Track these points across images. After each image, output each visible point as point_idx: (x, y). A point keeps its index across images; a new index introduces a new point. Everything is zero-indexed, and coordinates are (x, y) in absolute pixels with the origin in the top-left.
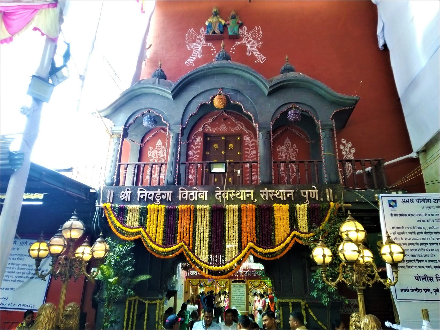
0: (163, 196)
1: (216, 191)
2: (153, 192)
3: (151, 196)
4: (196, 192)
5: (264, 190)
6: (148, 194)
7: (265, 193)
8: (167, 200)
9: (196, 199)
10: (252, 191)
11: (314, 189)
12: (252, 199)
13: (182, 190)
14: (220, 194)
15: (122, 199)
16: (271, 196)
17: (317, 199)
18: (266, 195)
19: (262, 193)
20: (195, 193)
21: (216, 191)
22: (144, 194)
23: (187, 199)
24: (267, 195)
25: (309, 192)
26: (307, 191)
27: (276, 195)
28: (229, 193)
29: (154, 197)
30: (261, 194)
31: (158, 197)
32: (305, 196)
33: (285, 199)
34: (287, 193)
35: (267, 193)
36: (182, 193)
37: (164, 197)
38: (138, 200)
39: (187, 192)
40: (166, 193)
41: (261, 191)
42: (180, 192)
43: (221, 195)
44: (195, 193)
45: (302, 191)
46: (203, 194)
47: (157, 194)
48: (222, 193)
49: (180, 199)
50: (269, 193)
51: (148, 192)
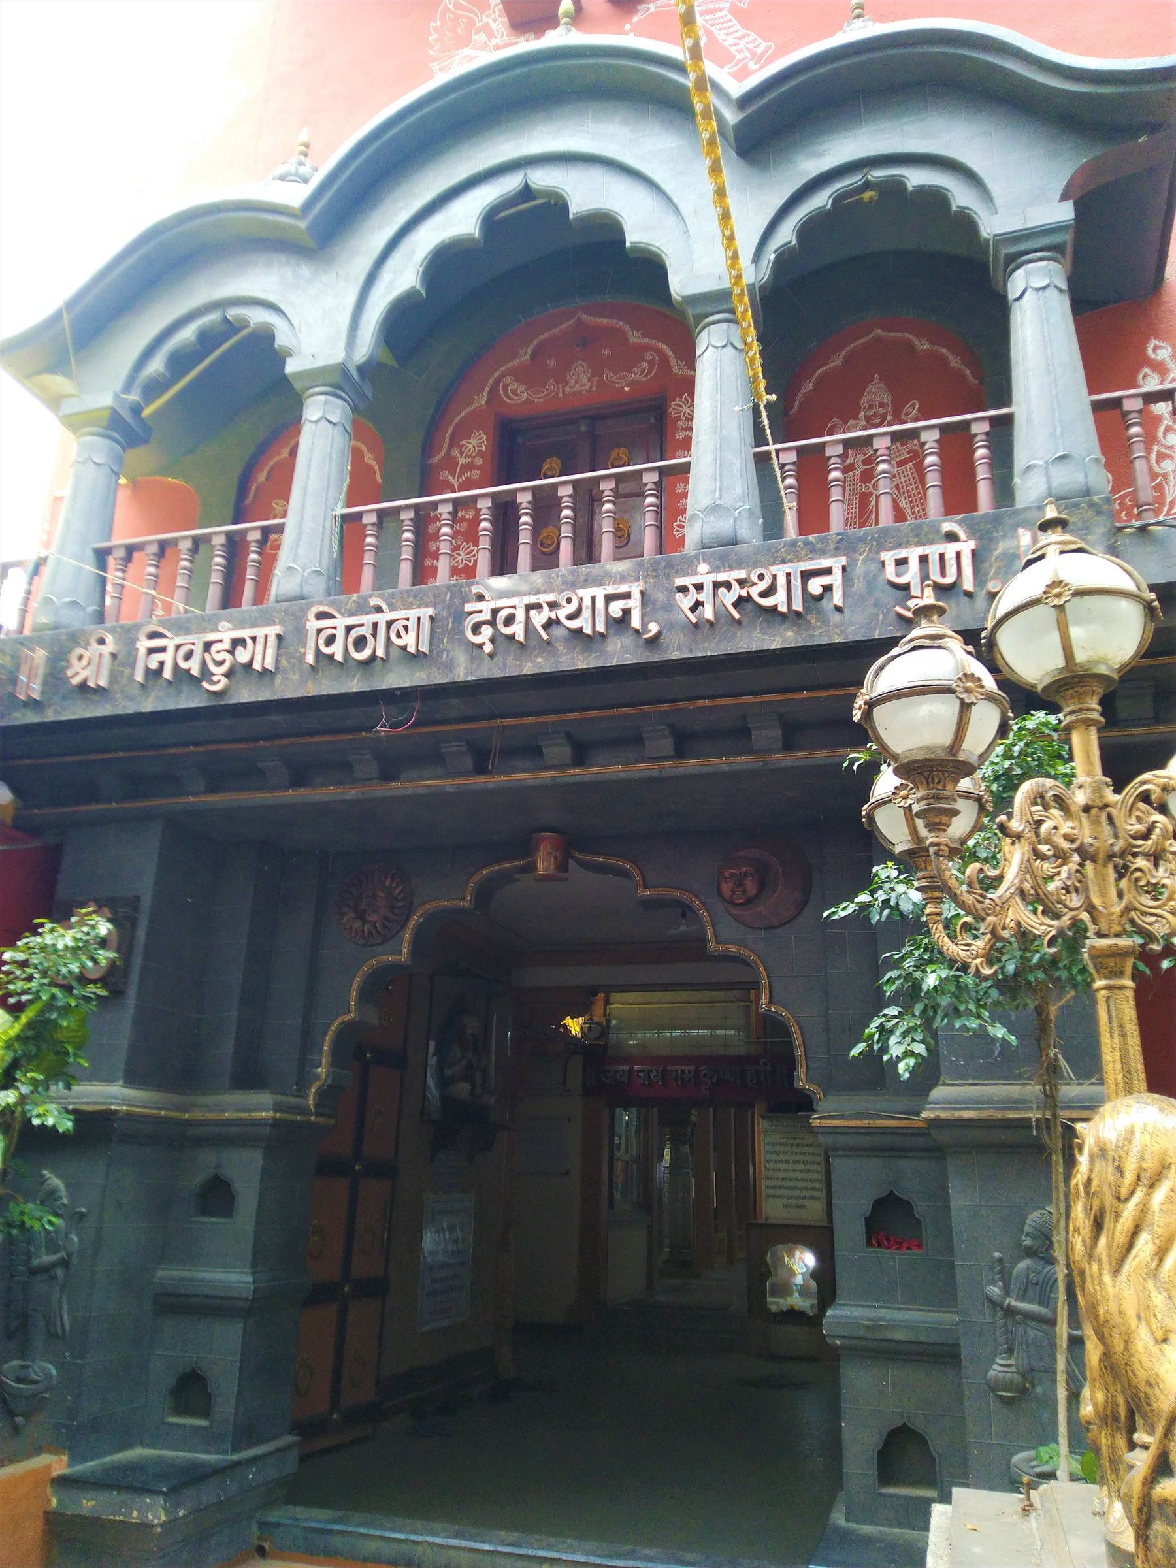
0: (239, 650)
1: (468, 607)
2: (199, 640)
3: (188, 656)
4: (382, 619)
5: (695, 573)
6: (178, 647)
7: (699, 587)
8: (257, 666)
9: (380, 653)
10: (636, 590)
11: (952, 537)
12: (636, 622)
13: (321, 616)
14: (486, 616)
15: (75, 681)
16: (727, 598)
17: (968, 584)
18: (701, 598)
19: (684, 589)
20: (375, 625)
21: (468, 607)
22: (163, 650)
23: (339, 657)
24: (706, 596)
25: (924, 559)
26: (913, 554)
27: (754, 592)
28: (529, 607)
29: (204, 663)
30: (679, 595)
31: (219, 657)
32: (902, 580)
33: (798, 606)
34: (807, 575)
35: (708, 588)
36: (319, 631)
37: (242, 656)
38: (139, 677)
39: (341, 622)
40: (254, 639)
41: (679, 582)
42: (313, 624)
43: (492, 623)
44: (375, 625)
45: (889, 557)
46: (412, 625)
47: (214, 648)
48: (495, 612)
49: (310, 659)
50: (716, 585)
51: (178, 641)
